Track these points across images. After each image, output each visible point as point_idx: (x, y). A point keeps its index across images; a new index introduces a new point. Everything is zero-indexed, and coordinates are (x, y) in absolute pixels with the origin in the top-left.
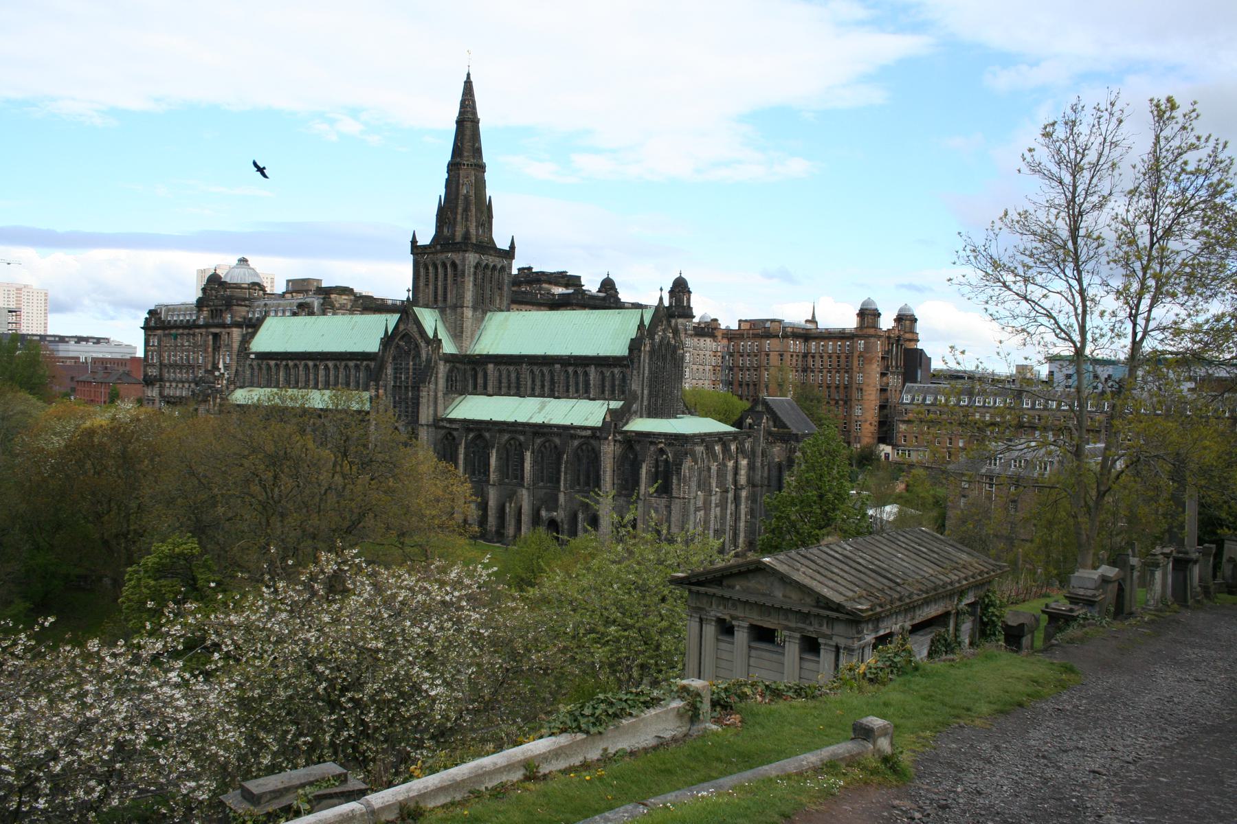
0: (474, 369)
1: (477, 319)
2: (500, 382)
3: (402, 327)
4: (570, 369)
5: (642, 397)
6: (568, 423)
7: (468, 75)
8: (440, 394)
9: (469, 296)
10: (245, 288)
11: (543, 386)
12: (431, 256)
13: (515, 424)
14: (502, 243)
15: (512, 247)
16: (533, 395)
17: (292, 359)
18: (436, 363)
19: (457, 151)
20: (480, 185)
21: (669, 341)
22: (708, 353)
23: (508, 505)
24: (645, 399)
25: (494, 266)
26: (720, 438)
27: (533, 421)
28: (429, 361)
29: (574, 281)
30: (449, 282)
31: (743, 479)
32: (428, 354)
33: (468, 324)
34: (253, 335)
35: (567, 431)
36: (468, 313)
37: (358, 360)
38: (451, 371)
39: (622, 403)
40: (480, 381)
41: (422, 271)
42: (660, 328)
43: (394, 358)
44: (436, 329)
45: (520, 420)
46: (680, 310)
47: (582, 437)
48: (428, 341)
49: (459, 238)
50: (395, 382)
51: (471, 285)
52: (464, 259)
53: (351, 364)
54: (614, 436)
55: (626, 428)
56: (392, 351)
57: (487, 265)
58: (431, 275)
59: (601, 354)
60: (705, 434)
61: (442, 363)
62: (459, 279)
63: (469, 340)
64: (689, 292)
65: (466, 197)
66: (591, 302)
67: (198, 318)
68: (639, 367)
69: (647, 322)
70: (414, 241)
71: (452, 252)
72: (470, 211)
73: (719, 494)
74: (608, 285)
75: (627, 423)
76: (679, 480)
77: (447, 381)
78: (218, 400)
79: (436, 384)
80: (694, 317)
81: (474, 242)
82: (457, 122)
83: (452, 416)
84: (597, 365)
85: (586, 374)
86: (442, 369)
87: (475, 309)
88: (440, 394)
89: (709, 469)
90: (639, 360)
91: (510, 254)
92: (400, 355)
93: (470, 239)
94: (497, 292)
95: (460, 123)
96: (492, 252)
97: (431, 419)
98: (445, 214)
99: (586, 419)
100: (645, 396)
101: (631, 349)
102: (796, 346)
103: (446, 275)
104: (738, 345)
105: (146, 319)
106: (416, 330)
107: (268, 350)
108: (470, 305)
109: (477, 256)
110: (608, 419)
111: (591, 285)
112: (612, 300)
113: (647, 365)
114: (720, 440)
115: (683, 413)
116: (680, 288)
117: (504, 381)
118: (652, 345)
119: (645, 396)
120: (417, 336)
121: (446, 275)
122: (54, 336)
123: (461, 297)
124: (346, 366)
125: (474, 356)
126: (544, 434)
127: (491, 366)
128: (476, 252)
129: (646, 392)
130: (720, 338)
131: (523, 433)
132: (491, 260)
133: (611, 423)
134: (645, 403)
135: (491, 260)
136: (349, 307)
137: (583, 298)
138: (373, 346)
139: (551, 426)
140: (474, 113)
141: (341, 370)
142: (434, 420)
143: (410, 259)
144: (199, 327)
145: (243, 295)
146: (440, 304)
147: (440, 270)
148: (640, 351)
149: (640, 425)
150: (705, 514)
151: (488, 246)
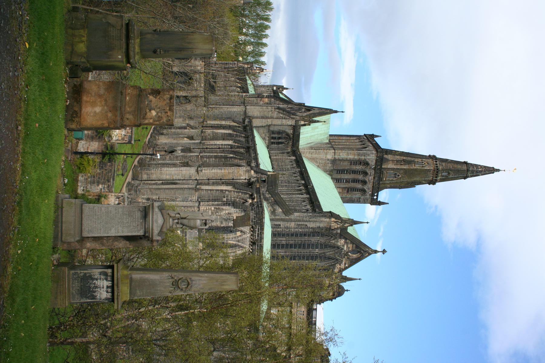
7: (498, 170)
15: (380, 203)
18: (292, 118)
25: (364, 182)
42: (350, 246)
51: (351, 157)
57: (365, 173)
70: (373, 136)
76: (218, 205)
77: (279, 133)
79: (277, 118)
81: (383, 167)
88: (269, 121)
91: (375, 202)
97: (250, 114)
100: (288, 224)
108: (337, 157)
113: (318, 225)
119: (288, 224)
128: (376, 160)
135: (368, 187)
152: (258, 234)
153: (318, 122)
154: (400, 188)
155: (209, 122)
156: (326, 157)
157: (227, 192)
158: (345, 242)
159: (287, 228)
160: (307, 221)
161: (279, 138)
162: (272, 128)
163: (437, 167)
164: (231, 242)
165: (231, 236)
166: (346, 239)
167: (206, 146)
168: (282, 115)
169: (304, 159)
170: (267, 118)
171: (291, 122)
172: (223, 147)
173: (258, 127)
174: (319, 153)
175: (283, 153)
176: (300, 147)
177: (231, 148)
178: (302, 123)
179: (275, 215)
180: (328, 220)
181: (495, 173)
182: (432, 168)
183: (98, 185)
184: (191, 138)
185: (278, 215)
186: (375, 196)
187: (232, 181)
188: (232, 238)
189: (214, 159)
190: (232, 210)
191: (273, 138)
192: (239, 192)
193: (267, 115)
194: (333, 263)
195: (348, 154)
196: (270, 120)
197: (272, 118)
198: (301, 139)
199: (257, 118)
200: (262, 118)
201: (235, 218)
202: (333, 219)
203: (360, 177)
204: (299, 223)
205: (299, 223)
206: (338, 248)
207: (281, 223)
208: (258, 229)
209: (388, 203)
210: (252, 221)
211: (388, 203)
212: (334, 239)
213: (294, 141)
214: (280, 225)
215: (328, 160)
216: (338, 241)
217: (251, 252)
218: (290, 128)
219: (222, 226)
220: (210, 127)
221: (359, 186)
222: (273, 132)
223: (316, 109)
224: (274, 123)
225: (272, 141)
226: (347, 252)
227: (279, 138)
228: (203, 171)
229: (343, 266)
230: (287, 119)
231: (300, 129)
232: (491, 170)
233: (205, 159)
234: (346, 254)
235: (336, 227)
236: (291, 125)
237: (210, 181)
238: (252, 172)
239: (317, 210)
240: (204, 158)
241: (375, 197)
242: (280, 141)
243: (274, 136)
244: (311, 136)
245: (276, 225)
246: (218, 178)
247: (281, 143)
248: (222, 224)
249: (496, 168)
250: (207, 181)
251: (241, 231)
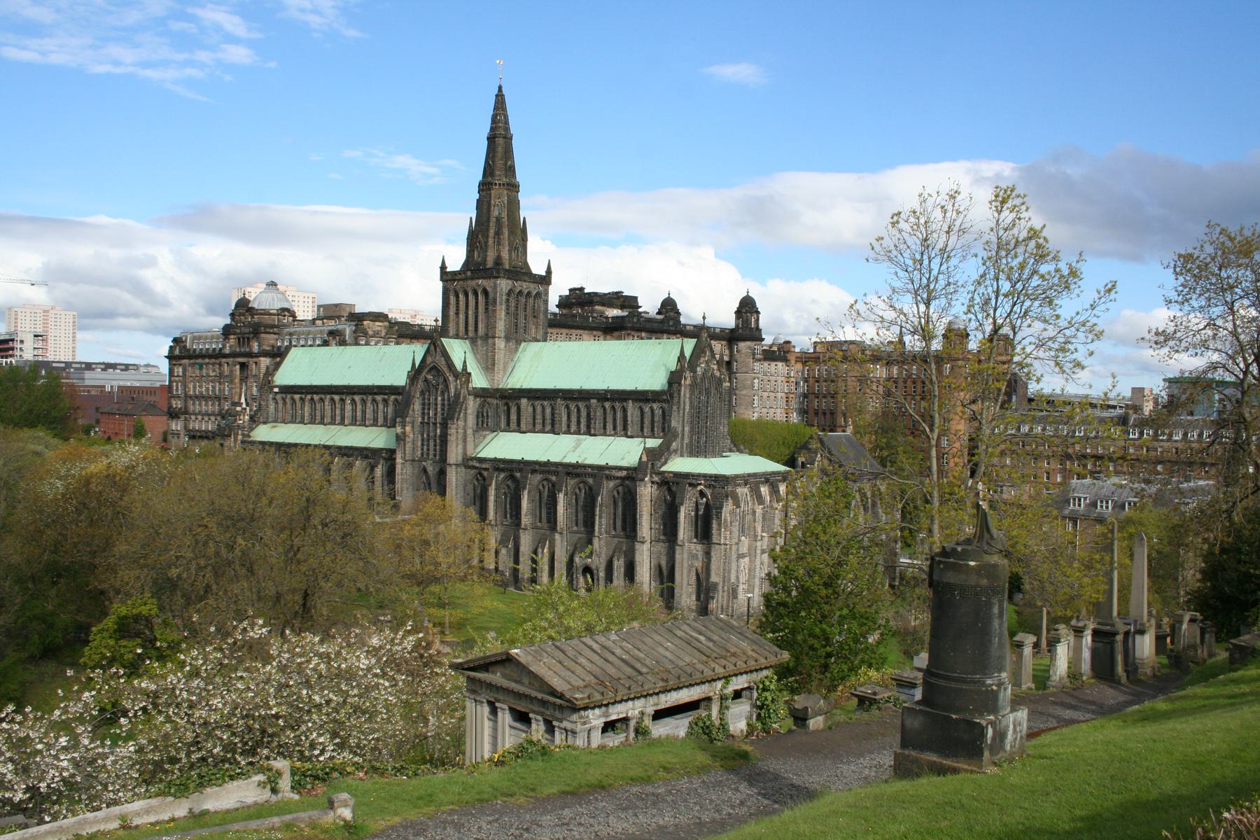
0: (507, 404)
1: (510, 350)
2: (534, 418)
3: (429, 360)
4: (607, 405)
5: (683, 435)
6: (603, 463)
7: (500, 88)
8: (470, 432)
9: (501, 326)
10: (274, 315)
11: (579, 422)
12: (461, 282)
13: (548, 463)
14: (538, 269)
15: (549, 271)
16: (568, 432)
17: (317, 393)
18: (465, 398)
19: (489, 170)
20: (513, 206)
21: (713, 375)
22: (780, 379)
24: (686, 436)
25: (529, 294)
26: (768, 478)
27: (567, 460)
28: (457, 395)
29: (629, 303)
30: (480, 310)
32: (456, 389)
33: (500, 356)
34: (278, 365)
35: (601, 472)
36: (500, 344)
37: (385, 394)
38: (482, 406)
39: (660, 441)
40: (514, 417)
41: (452, 299)
42: (702, 359)
43: (422, 393)
44: (465, 362)
45: (553, 459)
46: (748, 332)
47: (618, 478)
48: (457, 375)
49: (490, 264)
50: (423, 418)
51: (503, 313)
52: (495, 287)
53: (379, 398)
54: (651, 476)
55: (664, 469)
56: (420, 385)
57: (520, 292)
58: (461, 303)
59: (640, 388)
60: (749, 475)
61: (471, 398)
62: (490, 307)
63: (501, 373)
64: (758, 313)
65: (498, 220)
66: (648, 325)
67: (224, 346)
68: (679, 402)
69: (688, 354)
70: (443, 267)
71: (483, 278)
72: (502, 234)
73: (766, 539)
74: (669, 306)
75: (665, 463)
77: (478, 417)
78: (240, 437)
79: (465, 421)
80: (763, 340)
82: (488, 139)
83: (484, 454)
84: (635, 400)
85: (625, 410)
86: (472, 405)
87: (508, 339)
88: (470, 432)
89: (754, 512)
90: (679, 394)
91: (546, 280)
92: (429, 388)
93: (502, 264)
94: (530, 319)
95: (491, 139)
96: (526, 278)
97: (460, 458)
98: (476, 239)
99: (623, 459)
101: (670, 383)
102: (879, 371)
103: (477, 303)
104: (814, 370)
105: (171, 347)
106: (444, 362)
107: (292, 383)
108: (503, 335)
109: (510, 282)
110: (645, 459)
111: (649, 305)
113: (687, 400)
114: (767, 481)
115: (731, 451)
116: (747, 307)
117: (539, 417)
118: (694, 378)
120: (445, 370)
121: (477, 303)
122: (81, 363)
123: (491, 326)
124: (374, 400)
125: (506, 390)
126: (577, 475)
127: (524, 401)
128: (508, 278)
129: (687, 429)
130: (793, 362)
131: (556, 473)
132: (525, 286)
133: (647, 463)
134: (686, 441)
135: (525, 286)
136: (383, 334)
137: (638, 320)
138: (400, 379)
139: (585, 466)
140: (507, 129)
141: (369, 404)
142: (463, 459)
143: (438, 286)
144: (225, 356)
145: (271, 322)
146: (471, 334)
147: (471, 297)
148: (680, 384)
149: (679, 464)
150: (750, 561)
151: (521, 272)
174: (499, 360)
181: (504, 92)
195: (500, 319)
199: (465, 449)
200: (465, 441)
239: (665, 397)
249: (496, 92)
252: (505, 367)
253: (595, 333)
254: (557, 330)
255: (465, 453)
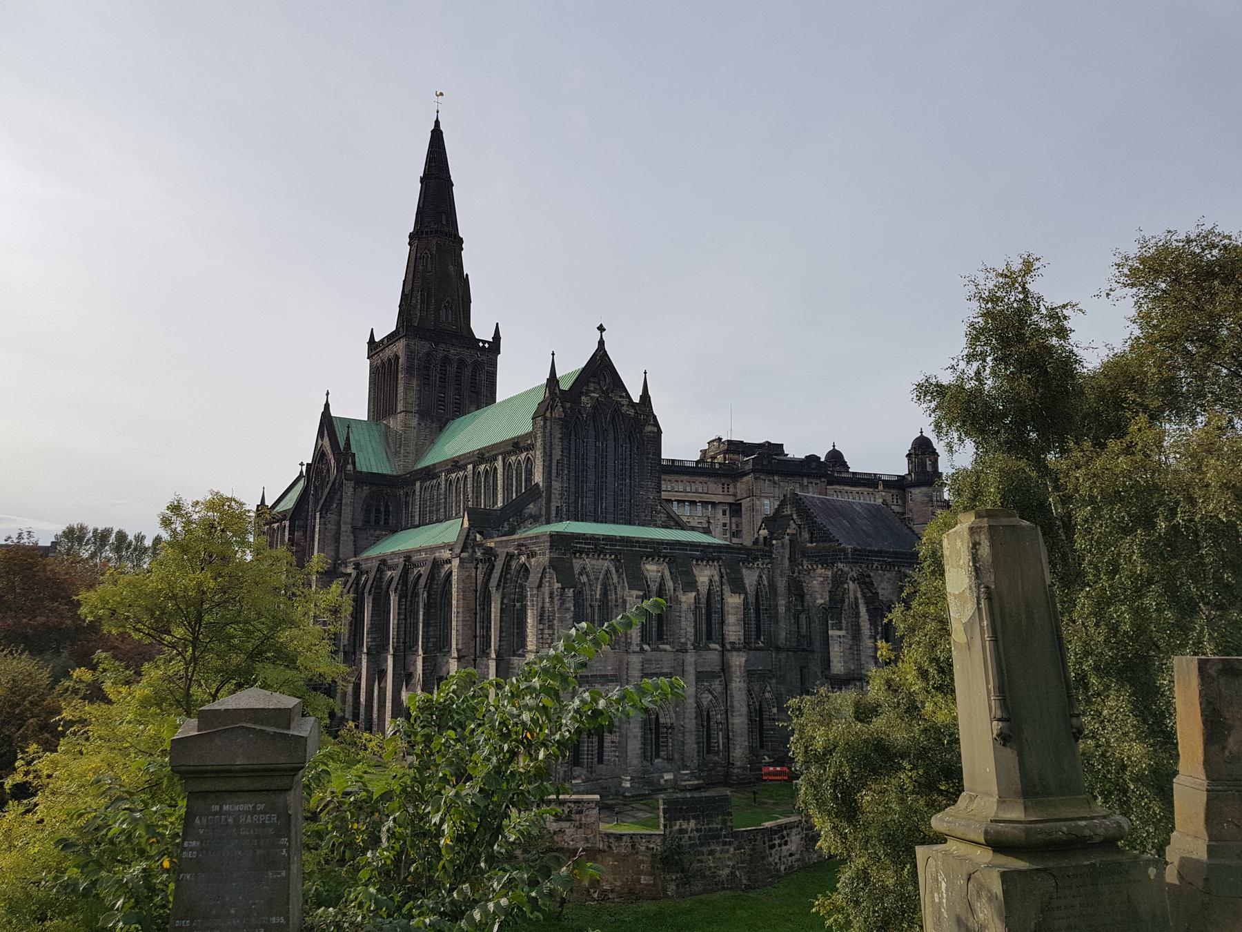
7: (437, 122)
23: (376, 683)
25: (462, 363)
31: (733, 631)
57: (446, 360)
70: (372, 341)
77: (367, 511)
89: (624, 601)
91: (495, 345)
112: (814, 465)
113: (556, 441)
152: (585, 544)
153: (348, 439)
154: (468, 301)
155: (346, 642)
156: (414, 428)
157: (505, 601)
158: (586, 394)
159: (562, 494)
160: (551, 461)
161: (378, 510)
162: (360, 524)
163: (432, 232)
164: (598, 592)
165: (587, 591)
166: (582, 393)
167: (401, 644)
168: (335, 505)
169: (419, 467)
170: (338, 532)
171: (349, 488)
172: (403, 611)
173: (355, 548)
175: (407, 503)
176: (395, 473)
177: (406, 597)
178: (350, 467)
179: (540, 515)
180: (548, 423)
182: (434, 241)
183: (516, 857)
184: (382, 673)
185: (540, 509)
186: (484, 346)
187: (480, 593)
188: (592, 590)
189: (431, 628)
190: (546, 590)
191: (377, 522)
192: (506, 579)
193: (334, 532)
194: (621, 418)
196: (342, 525)
197: (338, 524)
198: (380, 472)
200: (337, 541)
201: (560, 585)
202: (548, 414)
203: (452, 370)
204: (554, 474)
205: (554, 471)
206: (594, 407)
207: (554, 505)
208: (577, 543)
209: (497, 324)
210: (564, 554)
211: (497, 324)
212: (581, 414)
213: (385, 483)
214: (558, 507)
215: (419, 424)
216: (585, 408)
217: (616, 556)
218: (359, 490)
219: (572, 609)
220: (355, 639)
221: (468, 372)
222: (367, 522)
223: (320, 441)
224: (349, 520)
225: (382, 523)
226: (603, 391)
227: (378, 510)
228: (460, 647)
229: (625, 402)
230: (342, 495)
231: (361, 472)
232: (437, 137)
233: (430, 645)
234: (605, 393)
235: (561, 409)
236: (354, 488)
237: (478, 634)
238: (464, 555)
240: (428, 647)
241: (487, 345)
242: (382, 509)
243: (373, 520)
244: (374, 453)
245: (557, 514)
246: (473, 620)
247: (387, 506)
248: (569, 609)
249: (432, 127)
250: (478, 639)
251: (581, 574)
252: (417, 450)
253: (723, 480)
254: (676, 477)
255: (337, 557)
